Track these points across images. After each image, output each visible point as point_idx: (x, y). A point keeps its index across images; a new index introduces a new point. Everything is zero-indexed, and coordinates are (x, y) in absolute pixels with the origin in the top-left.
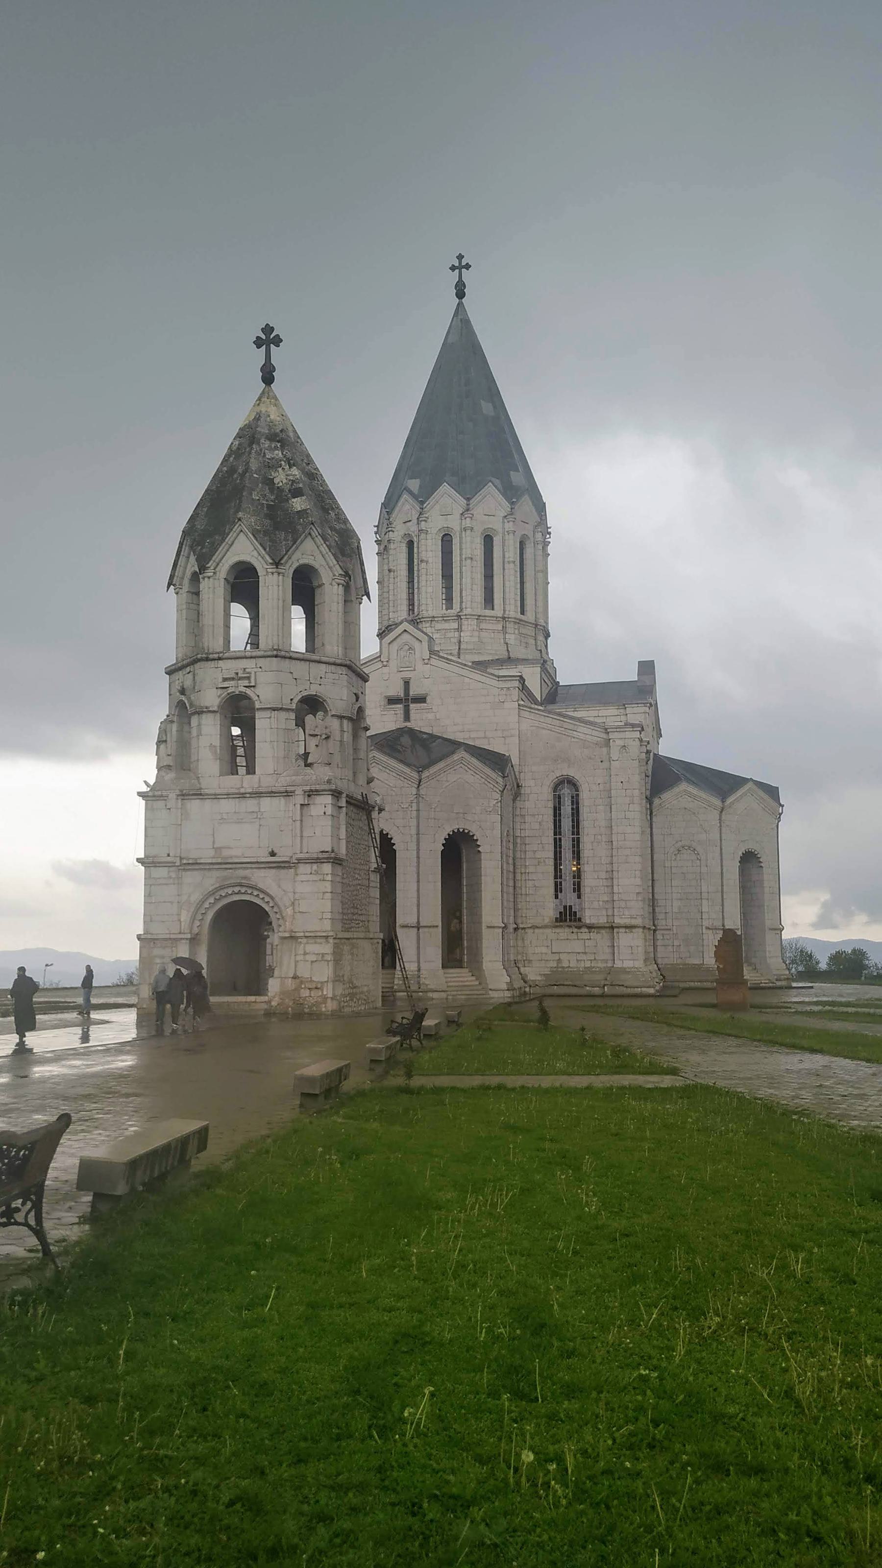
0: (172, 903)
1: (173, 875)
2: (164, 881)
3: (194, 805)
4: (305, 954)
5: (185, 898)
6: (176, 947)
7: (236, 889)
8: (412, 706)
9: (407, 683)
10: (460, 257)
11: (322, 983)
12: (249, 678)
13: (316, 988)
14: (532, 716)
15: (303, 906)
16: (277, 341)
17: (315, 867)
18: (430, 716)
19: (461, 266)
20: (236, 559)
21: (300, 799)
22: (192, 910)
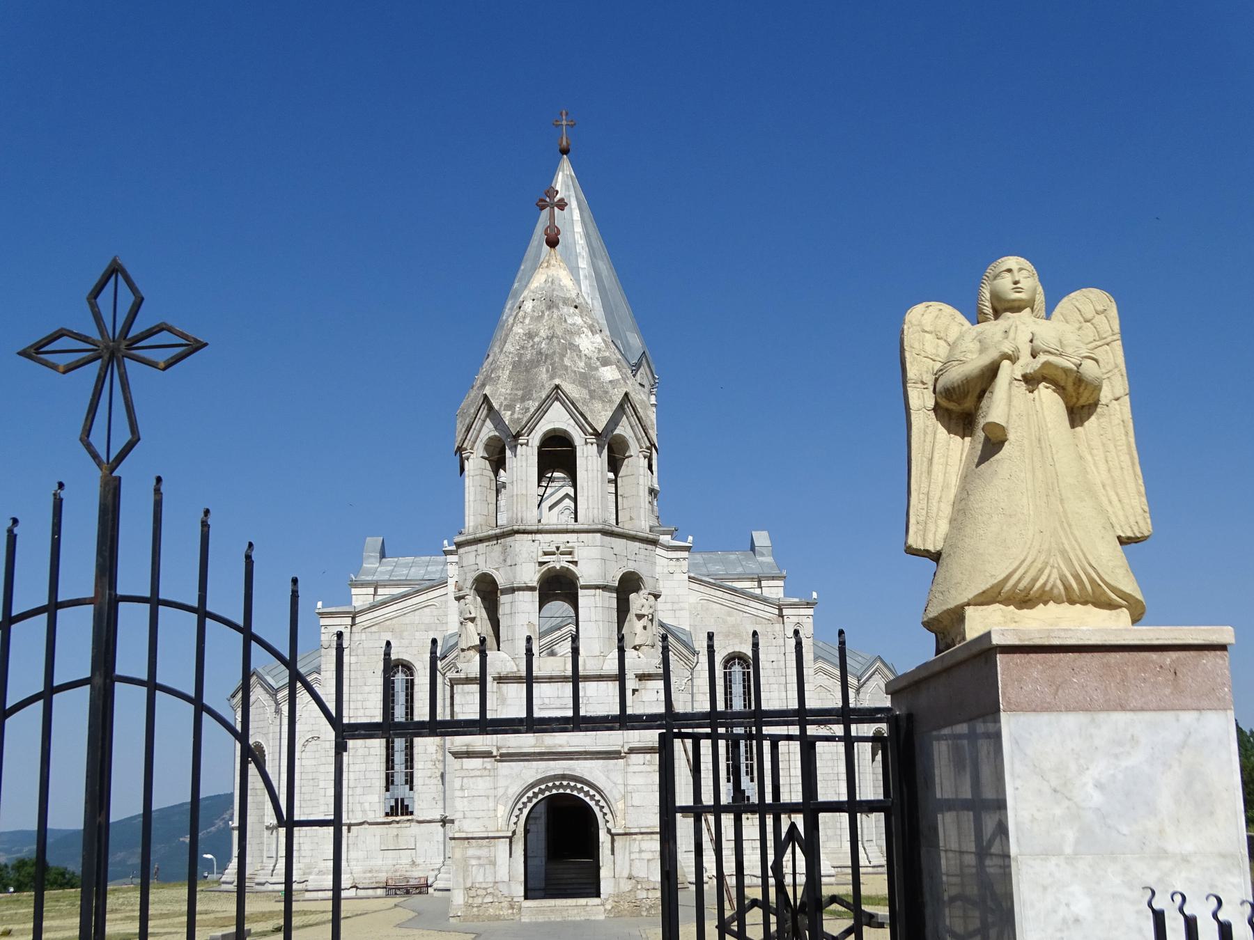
0: (488, 797)
1: (489, 766)
2: (478, 773)
4: (641, 851)
5: (500, 791)
14: (702, 588)
22: (510, 803)
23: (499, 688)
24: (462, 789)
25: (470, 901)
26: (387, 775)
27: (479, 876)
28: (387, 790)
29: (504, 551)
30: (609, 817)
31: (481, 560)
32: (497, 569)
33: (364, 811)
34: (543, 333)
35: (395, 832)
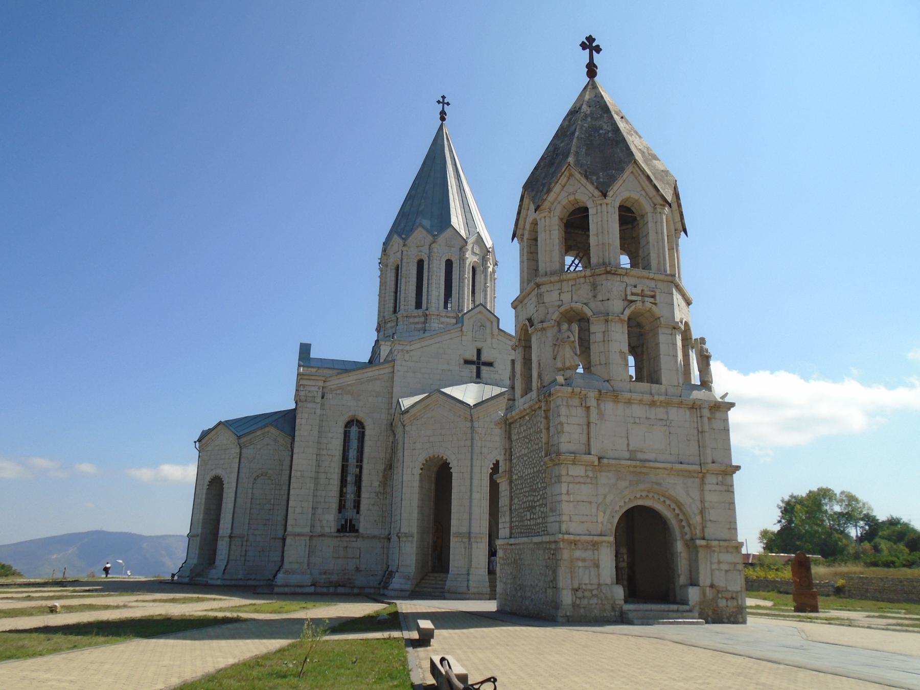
1: (590, 474)
2: (582, 480)
3: (608, 407)
4: (719, 562)
5: (601, 499)
6: (597, 550)
7: (644, 494)
8: (484, 369)
9: (479, 351)
10: (443, 97)
11: (737, 592)
12: (653, 297)
13: (732, 598)
15: (712, 515)
16: (598, 49)
17: (720, 478)
18: (497, 377)
19: (443, 102)
20: (626, 195)
21: (706, 412)
22: (608, 511)
23: (598, 405)
24: (568, 493)
25: (578, 602)
26: (340, 501)
27: (585, 577)
28: (340, 512)
29: (594, 287)
30: (687, 529)
31: (566, 298)
32: (586, 304)
33: (322, 527)
34: (607, 127)
35: (345, 544)
